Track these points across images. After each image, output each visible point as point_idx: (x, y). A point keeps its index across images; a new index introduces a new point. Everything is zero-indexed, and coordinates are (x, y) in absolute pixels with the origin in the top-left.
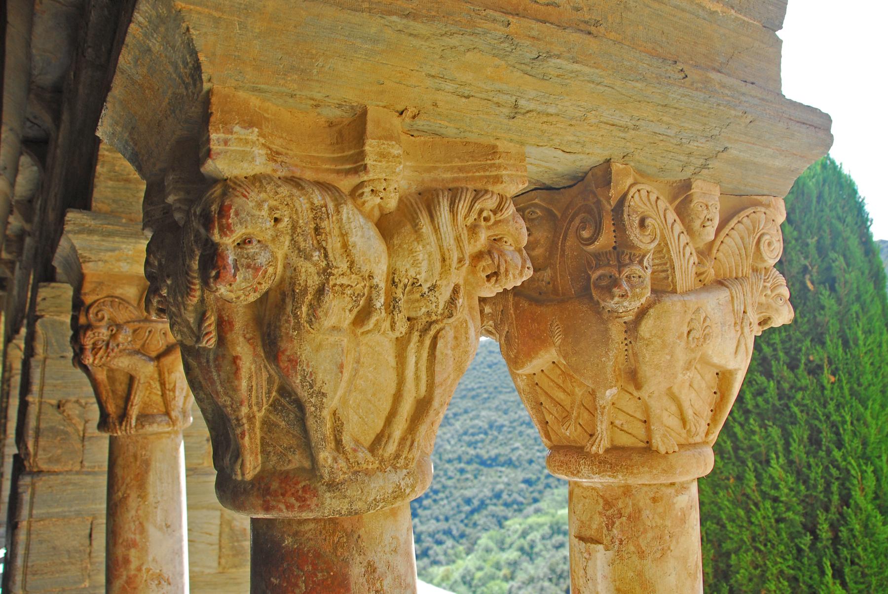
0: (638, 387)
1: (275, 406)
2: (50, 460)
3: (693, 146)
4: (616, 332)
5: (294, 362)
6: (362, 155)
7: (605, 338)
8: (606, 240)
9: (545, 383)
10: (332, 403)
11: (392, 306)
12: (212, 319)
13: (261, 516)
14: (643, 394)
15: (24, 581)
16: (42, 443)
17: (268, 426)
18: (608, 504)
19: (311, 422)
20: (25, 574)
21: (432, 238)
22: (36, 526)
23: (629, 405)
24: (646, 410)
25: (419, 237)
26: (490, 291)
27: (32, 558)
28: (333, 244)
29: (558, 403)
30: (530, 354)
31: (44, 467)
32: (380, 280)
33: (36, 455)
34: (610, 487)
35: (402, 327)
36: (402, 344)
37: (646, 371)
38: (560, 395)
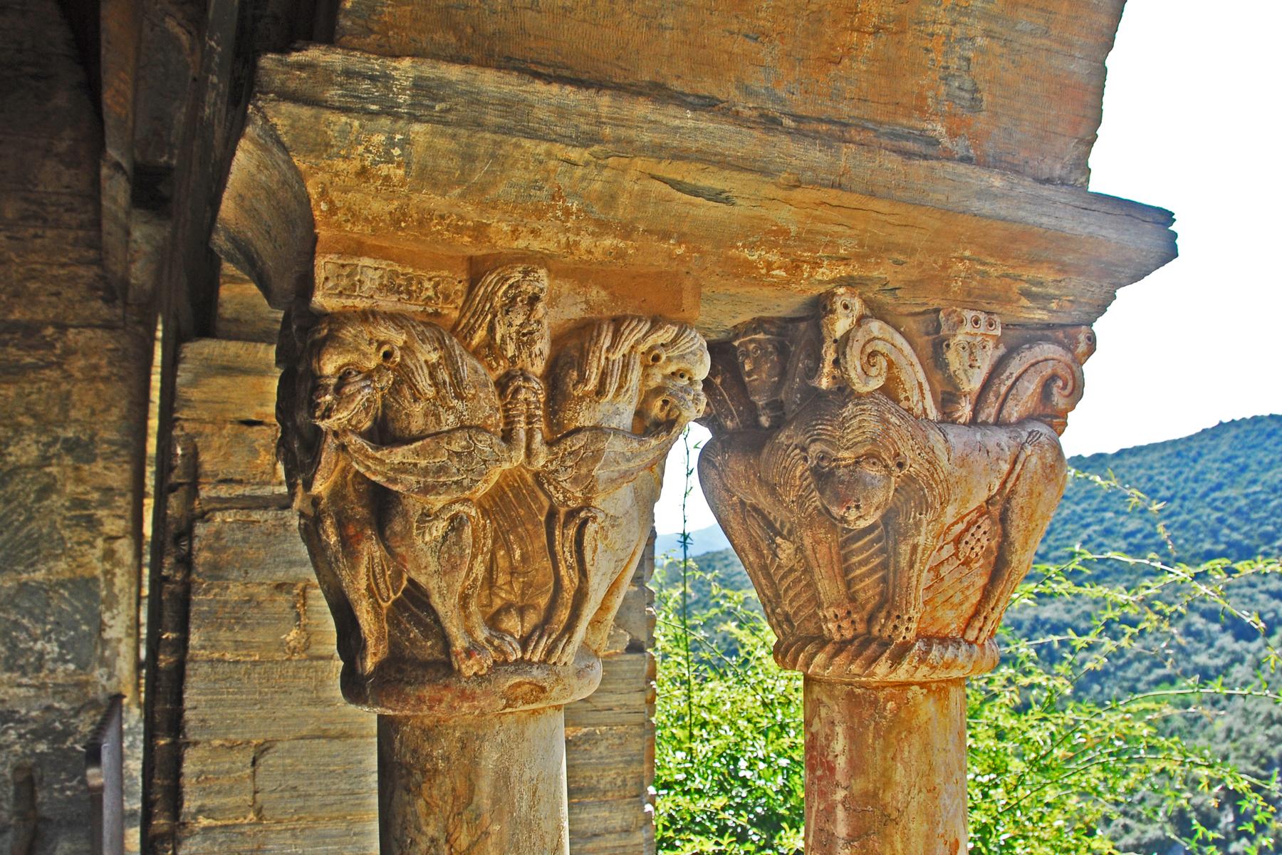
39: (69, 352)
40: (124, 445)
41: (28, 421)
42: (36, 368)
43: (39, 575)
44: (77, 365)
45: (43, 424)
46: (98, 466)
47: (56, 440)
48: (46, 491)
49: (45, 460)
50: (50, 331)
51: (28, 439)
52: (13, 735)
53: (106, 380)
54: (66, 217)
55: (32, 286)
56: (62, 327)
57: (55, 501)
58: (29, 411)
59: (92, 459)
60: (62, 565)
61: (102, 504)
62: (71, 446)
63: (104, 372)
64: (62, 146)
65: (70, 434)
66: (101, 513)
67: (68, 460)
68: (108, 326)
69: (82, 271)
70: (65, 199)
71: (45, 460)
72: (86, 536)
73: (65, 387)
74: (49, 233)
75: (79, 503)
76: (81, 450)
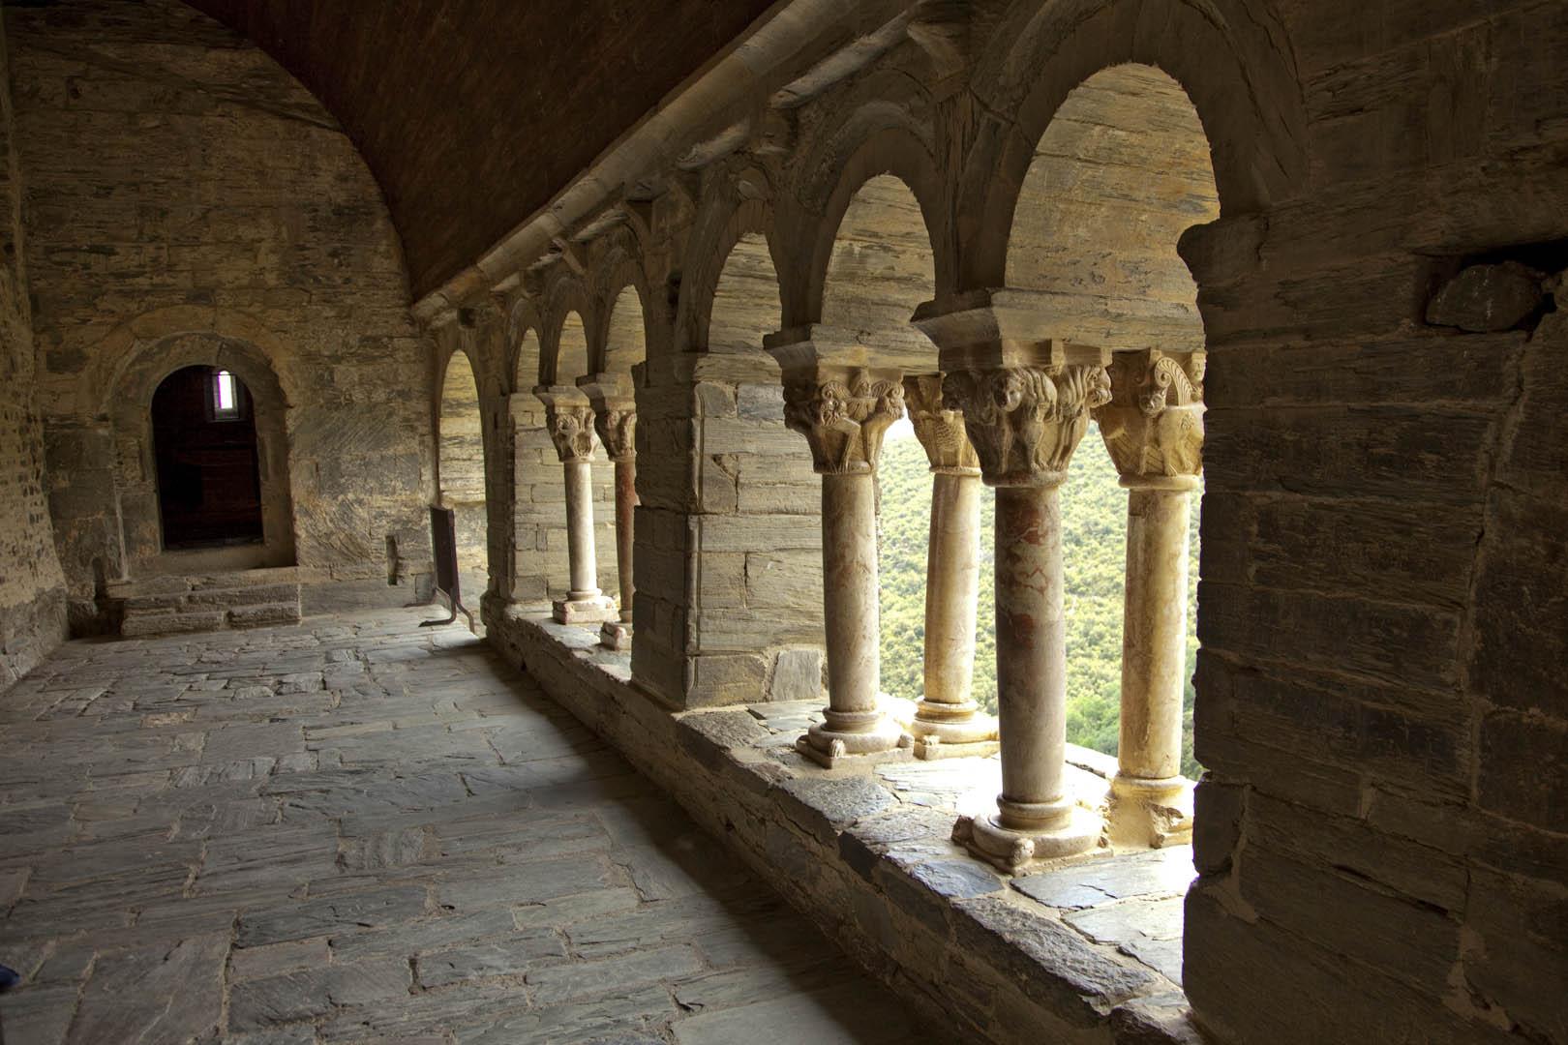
0: (1159, 446)
1: (1014, 447)
2: (712, 504)
3: (1192, 339)
4: (1149, 423)
5: (1025, 431)
6: (1050, 358)
7: (1144, 425)
8: (1146, 382)
9: (1119, 443)
10: (1036, 446)
11: (1058, 413)
12: (995, 415)
13: (1008, 486)
14: (1161, 449)
15: (699, 599)
16: (705, 489)
17: (1011, 454)
18: (1145, 498)
19: (1029, 453)
20: (699, 594)
21: (1073, 387)
22: (705, 556)
23: (1154, 453)
24: (1163, 456)
25: (1069, 387)
26: (1094, 406)
27: (703, 582)
28: (1040, 391)
29: (1124, 453)
30: (1112, 431)
31: (708, 509)
32: (1055, 403)
33: (701, 498)
34: (1146, 491)
35: (1061, 420)
36: (1060, 426)
37: (1162, 439)
38: (1125, 449)
39: (395, 350)
40: (425, 393)
41: (379, 382)
42: (381, 357)
43: (391, 452)
44: (400, 355)
45: (387, 384)
46: (414, 403)
47: (393, 391)
48: (390, 415)
49: (389, 400)
50: (385, 340)
51: (381, 390)
52: (384, 522)
53: (414, 362)
54: (388, 284)
55: (375, 318)
56: (391, 338)
57: (395, 419)
58: (379, 378)
59: (410, 399)
60: (400, 448)
61: (417, 420)
62: (400, 393)
63: (413, 359)
64: (382, 248)
65: (399, 388)
66: (416, 424)
67: (400, 400)
68: (412, 336)
69: (397, 310)
70: (387, 275)
71: (389, 400)
72: (411, 434)
73: (395, 366)
74: (380, 292)
75: (406, 420)
76: (404, 395)
